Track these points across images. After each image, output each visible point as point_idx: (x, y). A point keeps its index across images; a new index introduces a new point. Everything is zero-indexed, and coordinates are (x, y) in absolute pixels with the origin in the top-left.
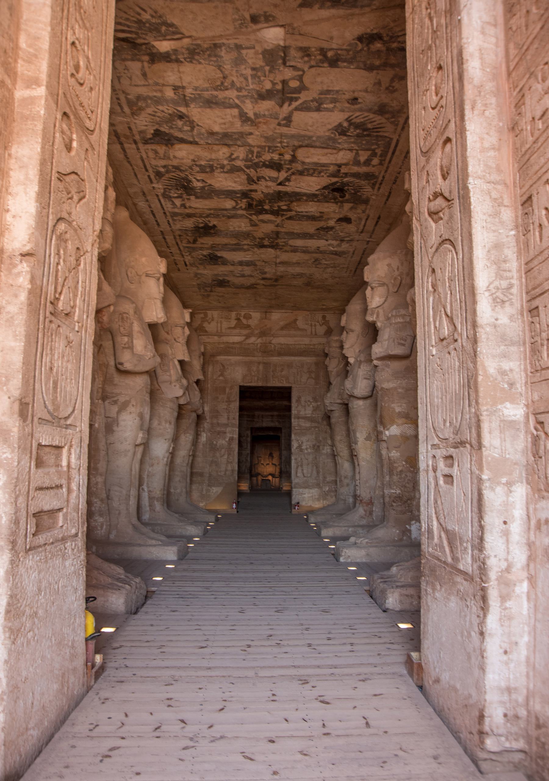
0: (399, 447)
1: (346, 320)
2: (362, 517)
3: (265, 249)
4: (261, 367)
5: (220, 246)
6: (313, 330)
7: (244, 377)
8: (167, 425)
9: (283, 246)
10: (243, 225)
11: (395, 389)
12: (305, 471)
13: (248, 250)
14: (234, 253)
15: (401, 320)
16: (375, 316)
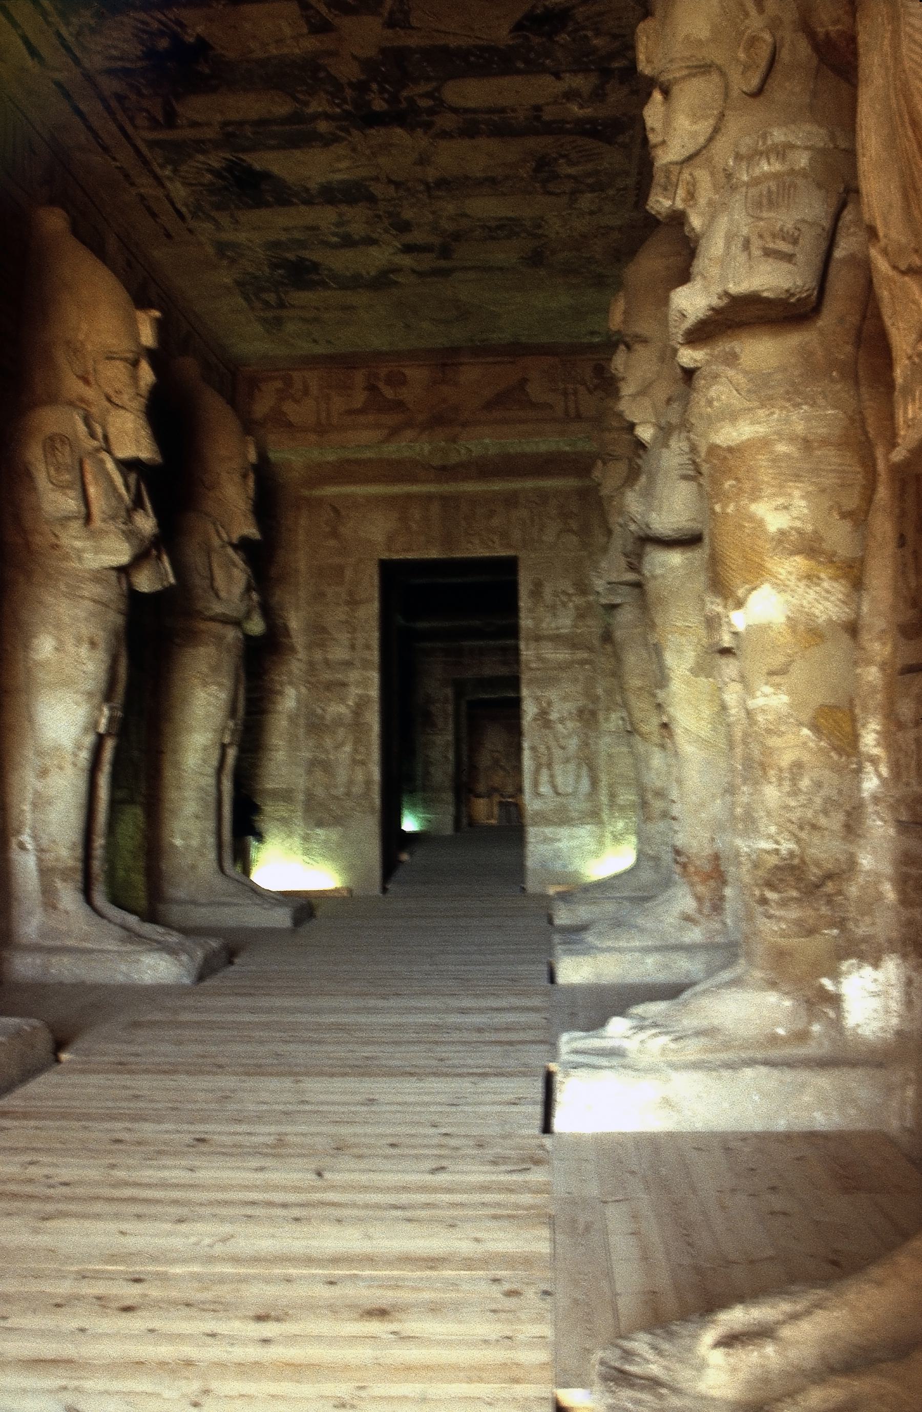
0: (782, 671)
1: (626, 312)
2: (687, 918)
3: (383, 131)
4: (435, 509)
5: (248, 131)
6: (572, 405)
7: (390, 539)
8: (84, 651)
9: (431, 111)
10: (288, 31)
11: (764, 443)
12: (559, 780)
13: (336, 139)
14: (297, 153)
15: (777, 166)
16: (681, 193)
